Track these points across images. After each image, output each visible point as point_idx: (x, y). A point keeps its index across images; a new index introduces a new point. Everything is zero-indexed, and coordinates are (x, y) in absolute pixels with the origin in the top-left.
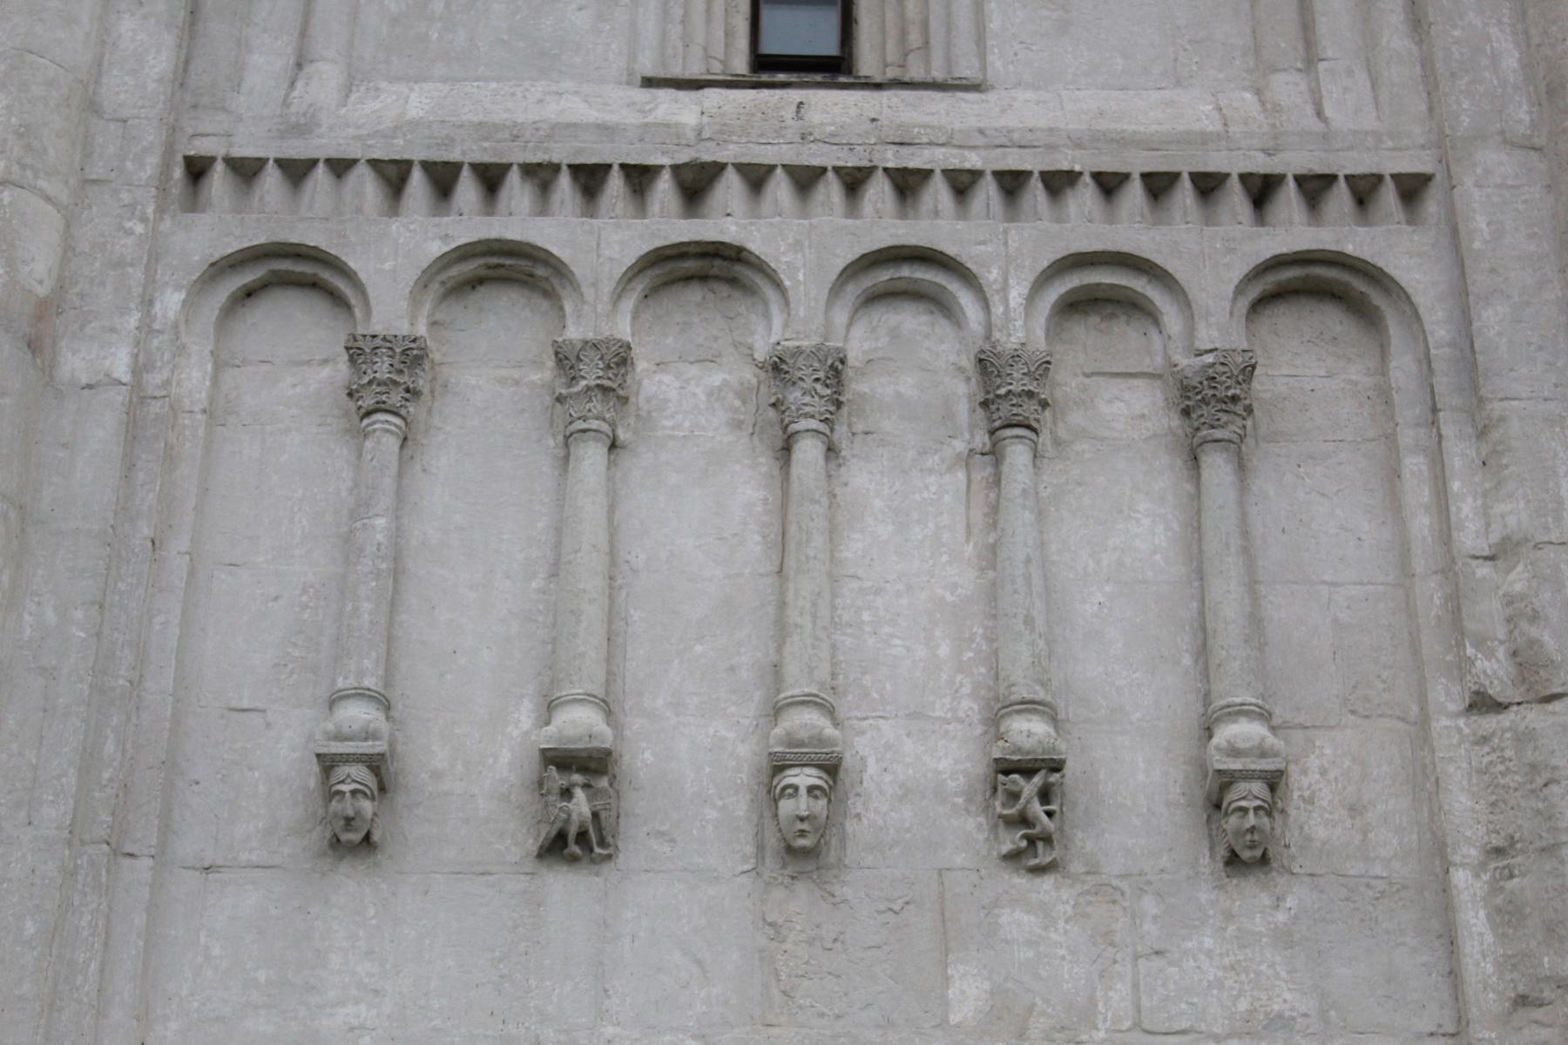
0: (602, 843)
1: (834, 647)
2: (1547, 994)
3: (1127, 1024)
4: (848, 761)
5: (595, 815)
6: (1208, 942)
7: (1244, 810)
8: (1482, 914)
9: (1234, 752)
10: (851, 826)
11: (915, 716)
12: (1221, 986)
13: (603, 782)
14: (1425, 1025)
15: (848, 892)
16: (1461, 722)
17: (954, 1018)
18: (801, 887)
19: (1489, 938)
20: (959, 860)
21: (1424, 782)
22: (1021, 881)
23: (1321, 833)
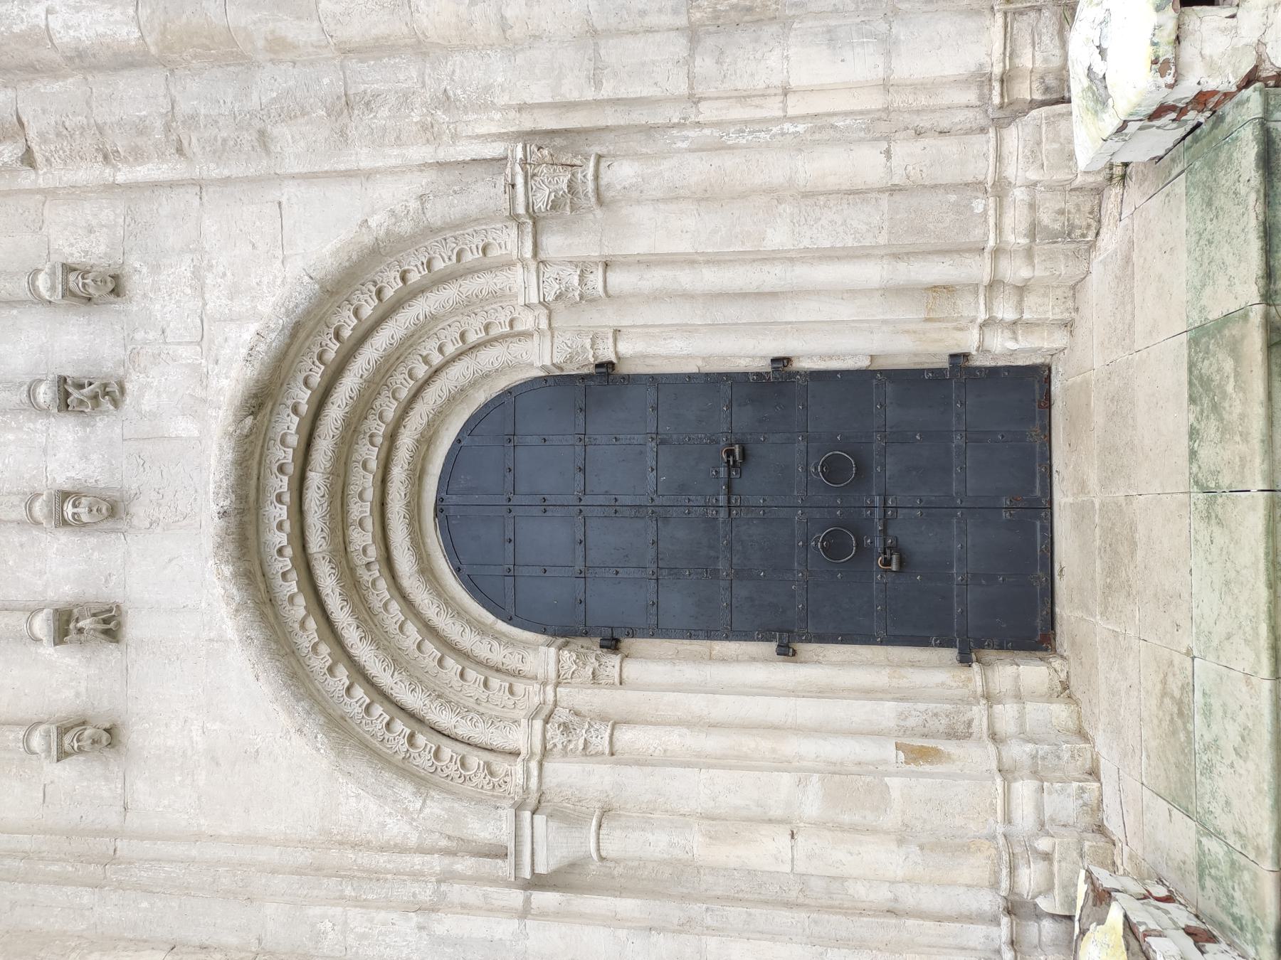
0: (110, 610)
4: (67, 487)
5: (94, 615)
6: (158, 307)
7: (84, 285)
8: (139, 168)
11: (45, 452)
12: (178, 301)
13: (75, 611)
15: (134, 486)
16: (41, 172)
17: (196, 434)
18: (133, 510)
19: (150, 166)
20: (118, 430)
21: (76, 193)
22: (128, 399)
23: (102, 248)
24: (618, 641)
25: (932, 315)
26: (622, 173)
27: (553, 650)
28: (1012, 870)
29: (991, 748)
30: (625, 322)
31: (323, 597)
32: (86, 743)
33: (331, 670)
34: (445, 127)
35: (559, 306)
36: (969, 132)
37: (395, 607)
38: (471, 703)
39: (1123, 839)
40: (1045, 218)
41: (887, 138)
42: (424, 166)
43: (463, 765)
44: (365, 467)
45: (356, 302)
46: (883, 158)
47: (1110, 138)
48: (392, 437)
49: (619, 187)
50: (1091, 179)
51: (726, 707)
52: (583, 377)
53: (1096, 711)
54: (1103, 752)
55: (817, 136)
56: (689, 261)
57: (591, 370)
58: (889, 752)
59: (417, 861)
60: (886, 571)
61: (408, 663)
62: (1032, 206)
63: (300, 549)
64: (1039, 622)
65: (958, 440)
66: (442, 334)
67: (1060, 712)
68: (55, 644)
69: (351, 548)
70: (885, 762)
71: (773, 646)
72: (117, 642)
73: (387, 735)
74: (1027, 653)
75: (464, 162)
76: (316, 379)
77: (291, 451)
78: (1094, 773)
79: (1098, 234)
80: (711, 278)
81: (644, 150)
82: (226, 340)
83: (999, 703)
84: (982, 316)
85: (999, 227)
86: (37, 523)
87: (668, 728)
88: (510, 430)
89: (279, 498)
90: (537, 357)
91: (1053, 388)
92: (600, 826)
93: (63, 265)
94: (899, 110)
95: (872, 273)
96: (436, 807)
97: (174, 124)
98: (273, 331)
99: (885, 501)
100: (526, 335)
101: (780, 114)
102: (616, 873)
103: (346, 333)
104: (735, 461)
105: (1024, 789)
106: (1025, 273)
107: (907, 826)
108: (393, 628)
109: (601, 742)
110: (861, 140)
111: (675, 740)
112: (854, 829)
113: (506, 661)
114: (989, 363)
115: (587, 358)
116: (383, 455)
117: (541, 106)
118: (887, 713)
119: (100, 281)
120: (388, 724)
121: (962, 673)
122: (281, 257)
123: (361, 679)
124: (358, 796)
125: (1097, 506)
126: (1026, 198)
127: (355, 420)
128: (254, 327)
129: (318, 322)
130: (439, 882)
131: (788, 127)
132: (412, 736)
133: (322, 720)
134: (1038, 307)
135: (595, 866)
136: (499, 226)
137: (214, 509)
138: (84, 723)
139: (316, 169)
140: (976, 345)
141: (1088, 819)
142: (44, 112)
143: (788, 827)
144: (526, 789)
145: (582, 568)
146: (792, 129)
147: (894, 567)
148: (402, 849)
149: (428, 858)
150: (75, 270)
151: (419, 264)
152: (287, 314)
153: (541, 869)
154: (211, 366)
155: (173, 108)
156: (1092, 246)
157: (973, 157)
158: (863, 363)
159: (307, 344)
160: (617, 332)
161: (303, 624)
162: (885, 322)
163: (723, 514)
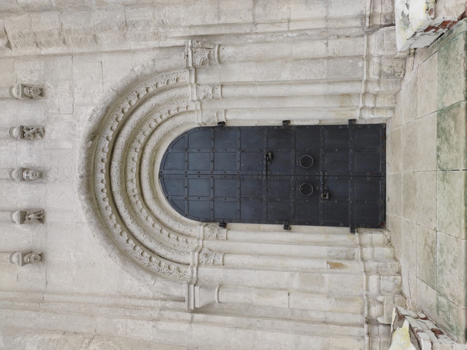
0: (40, 212)
1: (3, 169)
2: (62, 37)
3: (72, 116)
5: (35, 213)
6: (57, 100)
7: (30, 92)
9: (18, 93)
10: (37, 166)
11: (16, 153)
12: (64, 98)
13: (28, 212)
14: (71, 61)
15: (49, 166)
16: (13, 50)
17: (71, 147)
18: (48, 175)
19: (54, 48)
20: (43, 146)
21: (26, 58)
22: (46, 135)
23: (36, 79)
24: (226, 224)
25: (343, 105)
26: (228, 51)
27: (202, 227)
28: (369, 308)
29: (362, 264)
30: (229, 107)
31: (118, 207)
32: (32, 260)
33: (121, 234)
34: (162, 34)
35: (205, 101)
36: (357, 36)
37: (144, 211)
38: (172, 246)
39: (409, 297)
40: (385, 69)
41: (327, 39)
42: (155, 49)
43: (169, 268)
44: (133, 160)
45: (129, 99)
46: (325, 46)
47: (410, 38)
48: (143, 149)
49: (227, 57)
50: (402, 54)
51: (264, 248)
52: (213, 127)
53: (401, 250)
54: (403, 265)
55: (301, 38)
56: (253, 84)
57: (216, 125)
58: (324, 265)
59: (153, 303)
60: (324, 199)
61: (149, 231)
62: (380, 64)
63: (109, 190)
64: (380, 218)
65: (351, 151)
66: (161, 111)
67: (387, 251)
68: (21, 224)
69: (128, 190)
70: (323, 268)
71: (282, 226)
72: (43, 223)
73: (142, 257)
74: (376, 229)
75: (169, 47)
76: (115, 128)
77: (106, 154)
78: (399, 273)
79: (404, 75)
80: (261, 91)
81: (236, 43)
82: (82, 113)
83: (365, 247)
84: (361, 105)
85: (368, 72)
86: (13, 180)
87: (244, 256)
88: (186, 146)
89: (102, 171)
90: (196, 120)
91: (387, 132)
92: (219, 291)
93: (22, 85)
94: (331, 28)
95: (320, 89)
96: (159, 283)
97: (62, 32)
98: (99, 109)
99: (324, 174)
100: (192, 112)
101: (287, 29)
102: (224, 307)
103: (126, 110)
104: (269, 159)
105: (373, 279)
106: (377, 89)
107: (330, 291)
108: (143, 218)
109: (219, 261)
110: (317, 39)
111: (246, 260)
112: (311, 292)
113: (185, 231)
114: (363, 123)
115: (215, 120)
116: (140, 155)
117: (198, 26)
118: (324, 251)
119: (35, 91)
120: (142, 253)
121: (352, 236)
122: (102, 82)
123: (132, 237)
124: (131, 279)
125: (402, 176)
126: (378, 61)
127: (129, 142)
128: (92, 108)
129: (116, 107)
130: (160, 310)
131: (290, 34)
132: (150, 258)
133: (118, 252)
134: (382, 102)
135: (217, 305)
136: (182, 71)
137: (78, 175)
138: (31, 252)
139: (115, 49)
140: (358, 116)
141: (397, 289)
142: (14, 27)
143: (287, 291)
144: (192, 277)
145: (213, 197)
146: (291, 35)
147: (327, 198)
148: (147, 298)
149: (156, 302)
150: (26, 86)
151: (153, 85)
152: (104, 103)
153: (197, 306)
154: (76, 123)
155: (62, 26)
156: (402, 79)
157: (358, 46)
158: (316, 123)
159: (112, 114)
160: (226, 111)
161: (111, 217)
162: (324, 107)
163: (264, 178)
